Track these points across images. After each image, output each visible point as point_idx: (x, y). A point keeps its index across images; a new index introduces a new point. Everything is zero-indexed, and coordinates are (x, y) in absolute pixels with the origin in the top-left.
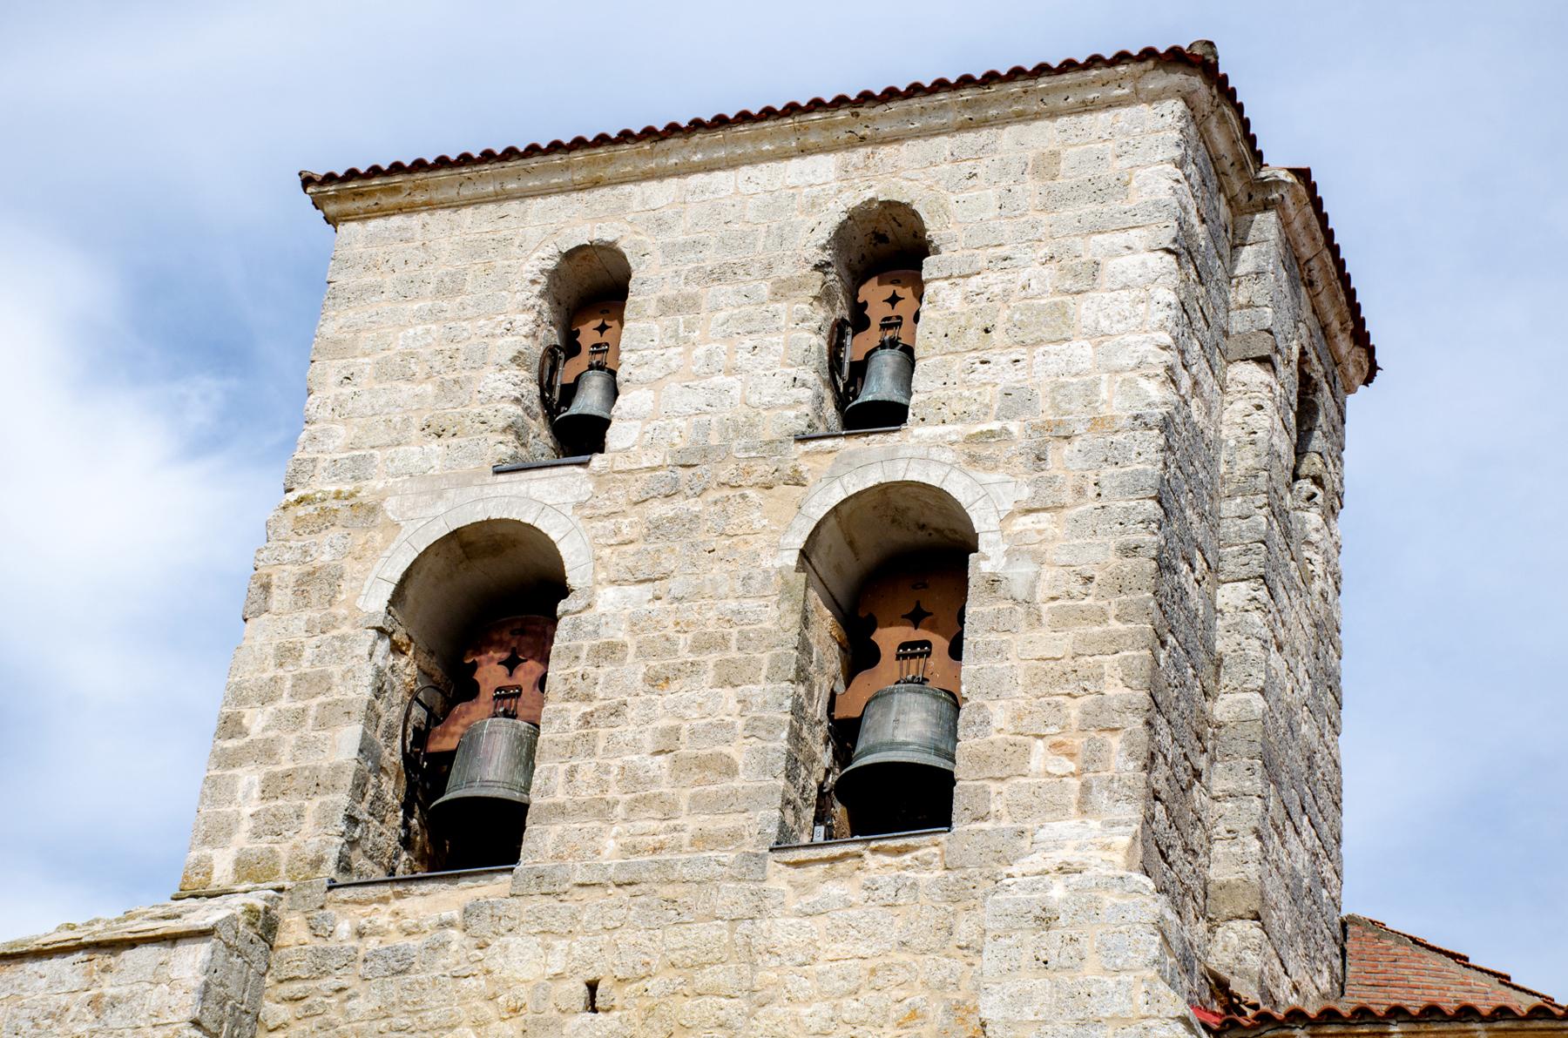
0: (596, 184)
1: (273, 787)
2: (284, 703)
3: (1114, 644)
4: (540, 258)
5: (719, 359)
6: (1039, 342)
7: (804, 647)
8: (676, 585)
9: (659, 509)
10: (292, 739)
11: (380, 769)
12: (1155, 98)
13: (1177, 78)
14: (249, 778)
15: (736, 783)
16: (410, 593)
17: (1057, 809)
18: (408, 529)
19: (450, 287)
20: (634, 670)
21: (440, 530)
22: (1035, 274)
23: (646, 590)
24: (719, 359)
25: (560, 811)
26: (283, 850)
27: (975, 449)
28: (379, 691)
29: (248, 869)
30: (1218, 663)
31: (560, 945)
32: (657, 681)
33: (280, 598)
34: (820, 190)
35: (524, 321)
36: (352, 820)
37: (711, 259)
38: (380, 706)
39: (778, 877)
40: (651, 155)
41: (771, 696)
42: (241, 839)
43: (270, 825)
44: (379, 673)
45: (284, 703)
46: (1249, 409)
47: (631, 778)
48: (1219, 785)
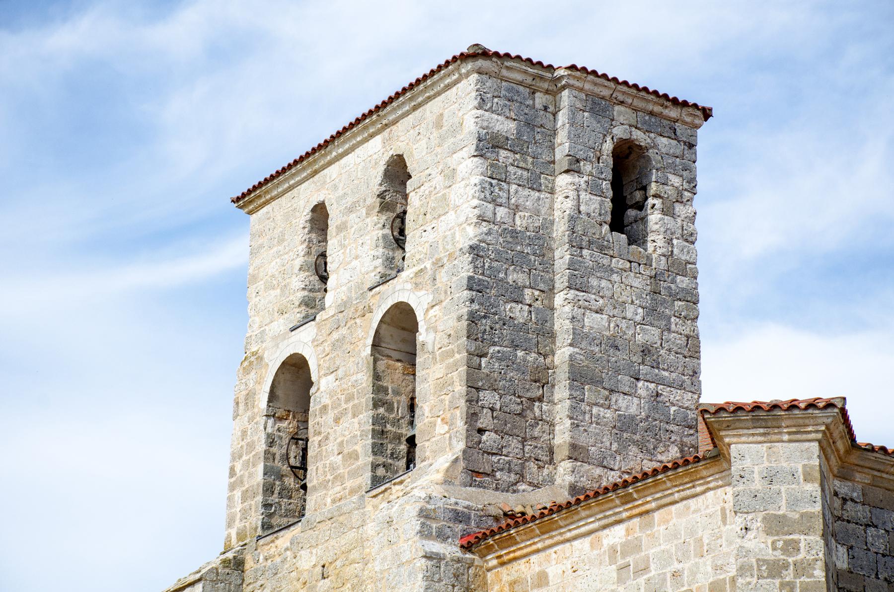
0: (316, 172)
1: (244, 499)
2: (245, 458)
3: (456, 365)
4: (304, 215)
5: (356, 251)
6: (439, 216)
7: (379, 390)
8: (340, 373)
9: (335, 335)
10: (246, 474)
11: (281, 477)
12: (467, 75)
13: (469, 66)
14: (238, 494)
15: (360, 462)
16: (279, 392)
17: (442, 451)
18: (270, 364)
19: (281, 241)
20: (331, 415)
21: (278, 364)
22: (438, 180)
23: (331, 378)
24: (356, 251)
25: (315, 488)
26: (247, 524)
27: (419, 280)
28: (271, 443)
29: (241, 536)
30: (552, 336)
31: (314, 551)
32: (337, 420)
33: (242, 407)
34: (367, 160)
35: (302, 248)
36: (267, 506)
37: (350, 200)
38: (274, 449)
39: (370, 503)
40: (325, 155)
41: (366, 416)
42: (238, 524)
43: (245, 513)
44: (269, 436)
45: (245, 458)
46: (571, 198)
47: (333, 468)
48: (557, 396)
